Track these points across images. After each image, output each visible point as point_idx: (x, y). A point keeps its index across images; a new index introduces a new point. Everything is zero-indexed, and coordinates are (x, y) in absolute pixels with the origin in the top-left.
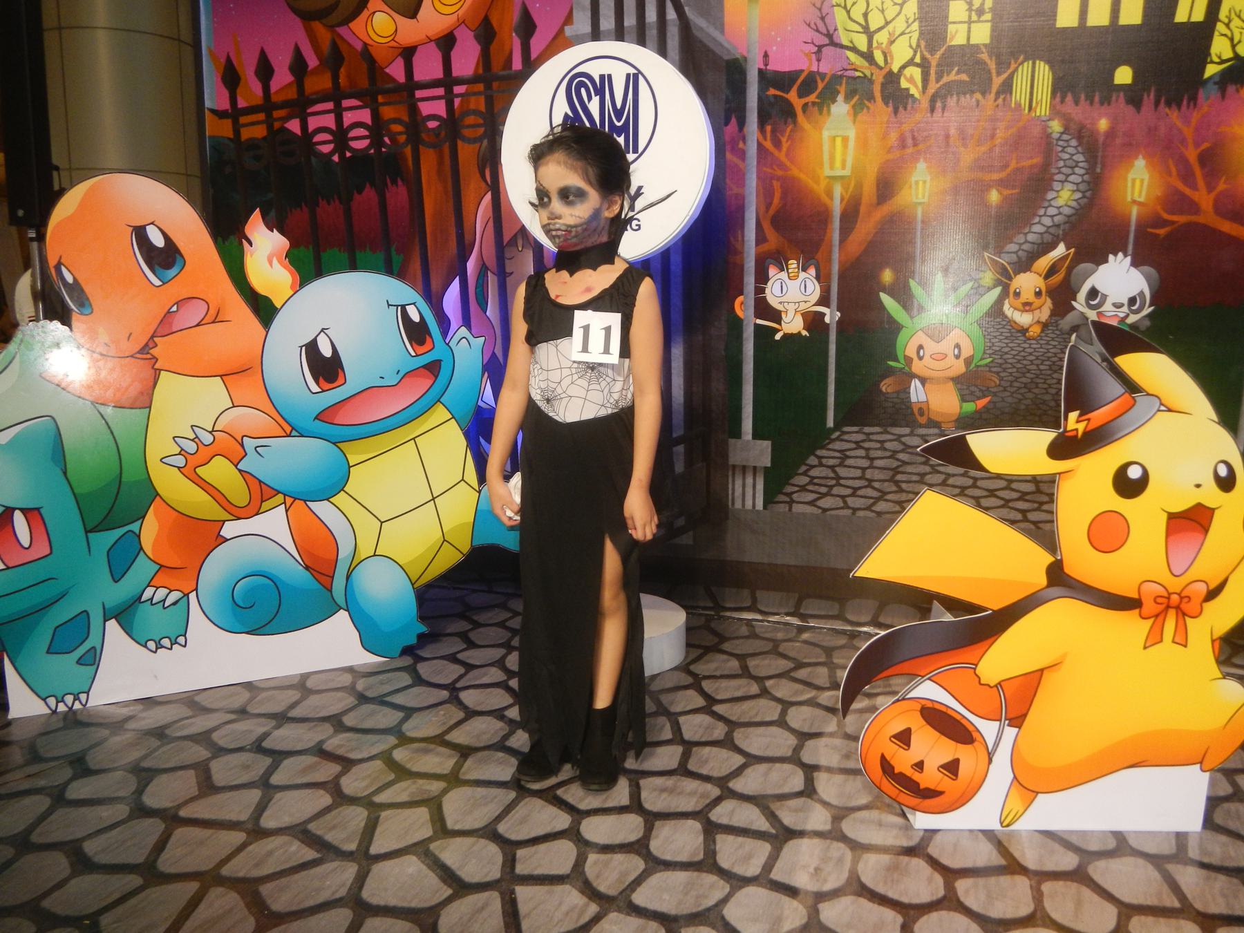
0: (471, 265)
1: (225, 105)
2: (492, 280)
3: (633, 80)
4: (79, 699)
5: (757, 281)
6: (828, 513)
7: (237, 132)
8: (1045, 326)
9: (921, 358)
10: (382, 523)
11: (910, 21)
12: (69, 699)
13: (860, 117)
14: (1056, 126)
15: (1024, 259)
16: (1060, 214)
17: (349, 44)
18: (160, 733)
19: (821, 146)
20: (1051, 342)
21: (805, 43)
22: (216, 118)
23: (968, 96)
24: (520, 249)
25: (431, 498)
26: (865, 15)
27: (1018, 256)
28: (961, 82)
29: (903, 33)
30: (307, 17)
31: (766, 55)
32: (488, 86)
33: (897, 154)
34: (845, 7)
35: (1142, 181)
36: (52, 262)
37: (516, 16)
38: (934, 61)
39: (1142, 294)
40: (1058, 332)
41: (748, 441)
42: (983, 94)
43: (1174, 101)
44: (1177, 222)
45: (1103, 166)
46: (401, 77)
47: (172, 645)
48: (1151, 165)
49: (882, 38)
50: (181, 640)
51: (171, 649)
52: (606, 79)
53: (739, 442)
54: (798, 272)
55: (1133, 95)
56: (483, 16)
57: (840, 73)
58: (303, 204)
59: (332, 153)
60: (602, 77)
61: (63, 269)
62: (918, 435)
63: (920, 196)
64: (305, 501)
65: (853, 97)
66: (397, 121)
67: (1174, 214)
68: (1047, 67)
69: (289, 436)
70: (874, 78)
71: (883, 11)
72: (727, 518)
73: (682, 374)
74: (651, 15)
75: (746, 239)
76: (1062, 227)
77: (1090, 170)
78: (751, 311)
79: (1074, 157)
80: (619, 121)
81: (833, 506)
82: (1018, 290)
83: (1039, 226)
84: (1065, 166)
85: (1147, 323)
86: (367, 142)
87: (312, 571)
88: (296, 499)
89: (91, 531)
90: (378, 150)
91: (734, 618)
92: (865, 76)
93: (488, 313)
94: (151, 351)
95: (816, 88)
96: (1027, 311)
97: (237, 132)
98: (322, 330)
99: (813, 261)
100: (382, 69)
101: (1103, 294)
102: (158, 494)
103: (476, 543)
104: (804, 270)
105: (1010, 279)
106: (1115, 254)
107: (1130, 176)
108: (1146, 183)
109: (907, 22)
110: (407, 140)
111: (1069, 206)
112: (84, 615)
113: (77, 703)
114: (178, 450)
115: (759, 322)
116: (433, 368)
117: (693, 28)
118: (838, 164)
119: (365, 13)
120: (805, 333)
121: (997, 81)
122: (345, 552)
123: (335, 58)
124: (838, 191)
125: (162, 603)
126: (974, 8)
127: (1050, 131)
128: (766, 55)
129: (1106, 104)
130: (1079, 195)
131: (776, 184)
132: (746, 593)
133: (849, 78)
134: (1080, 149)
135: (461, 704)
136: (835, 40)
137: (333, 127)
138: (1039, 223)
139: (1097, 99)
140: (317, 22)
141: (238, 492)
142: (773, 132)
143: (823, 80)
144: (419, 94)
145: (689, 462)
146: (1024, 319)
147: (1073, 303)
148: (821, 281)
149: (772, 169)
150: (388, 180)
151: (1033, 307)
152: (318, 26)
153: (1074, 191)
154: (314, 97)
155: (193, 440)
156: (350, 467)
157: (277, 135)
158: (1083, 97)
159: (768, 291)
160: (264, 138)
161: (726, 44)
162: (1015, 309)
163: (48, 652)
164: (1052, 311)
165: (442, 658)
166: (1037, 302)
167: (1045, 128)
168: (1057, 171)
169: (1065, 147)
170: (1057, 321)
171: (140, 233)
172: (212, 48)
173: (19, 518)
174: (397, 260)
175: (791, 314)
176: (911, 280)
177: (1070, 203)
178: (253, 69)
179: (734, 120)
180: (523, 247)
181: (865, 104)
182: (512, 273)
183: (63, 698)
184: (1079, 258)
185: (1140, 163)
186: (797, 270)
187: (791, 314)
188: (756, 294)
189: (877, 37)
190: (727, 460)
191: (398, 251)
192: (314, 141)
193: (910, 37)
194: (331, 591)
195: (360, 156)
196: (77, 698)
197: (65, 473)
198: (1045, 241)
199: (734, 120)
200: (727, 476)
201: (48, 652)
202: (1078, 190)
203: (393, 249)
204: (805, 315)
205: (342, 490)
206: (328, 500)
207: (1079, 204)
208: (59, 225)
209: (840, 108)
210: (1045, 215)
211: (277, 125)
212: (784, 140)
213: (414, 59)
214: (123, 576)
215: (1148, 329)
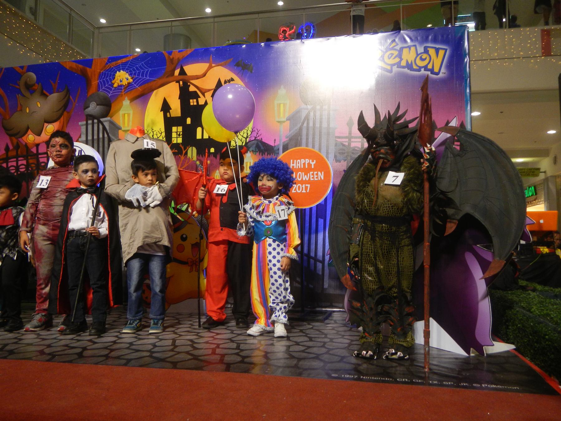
14: (198, 163)
26: (153, 136)
28: (176, 152)
30: (10, 136)
35: (218, 176)
42: (181, 155)
45: (209, 173)
46: (35, 152)
55: (215, 154)
59: (15, 172)
74: (101, 136)
86: (24, 169)
107: (216, 175)
119: (27, 135)
121: (184, 152)
123: (17, 147)
144: (40, 156)
150: (30, 180)
152: (14, 138)
195: (22, 173)
213: (39, 147)
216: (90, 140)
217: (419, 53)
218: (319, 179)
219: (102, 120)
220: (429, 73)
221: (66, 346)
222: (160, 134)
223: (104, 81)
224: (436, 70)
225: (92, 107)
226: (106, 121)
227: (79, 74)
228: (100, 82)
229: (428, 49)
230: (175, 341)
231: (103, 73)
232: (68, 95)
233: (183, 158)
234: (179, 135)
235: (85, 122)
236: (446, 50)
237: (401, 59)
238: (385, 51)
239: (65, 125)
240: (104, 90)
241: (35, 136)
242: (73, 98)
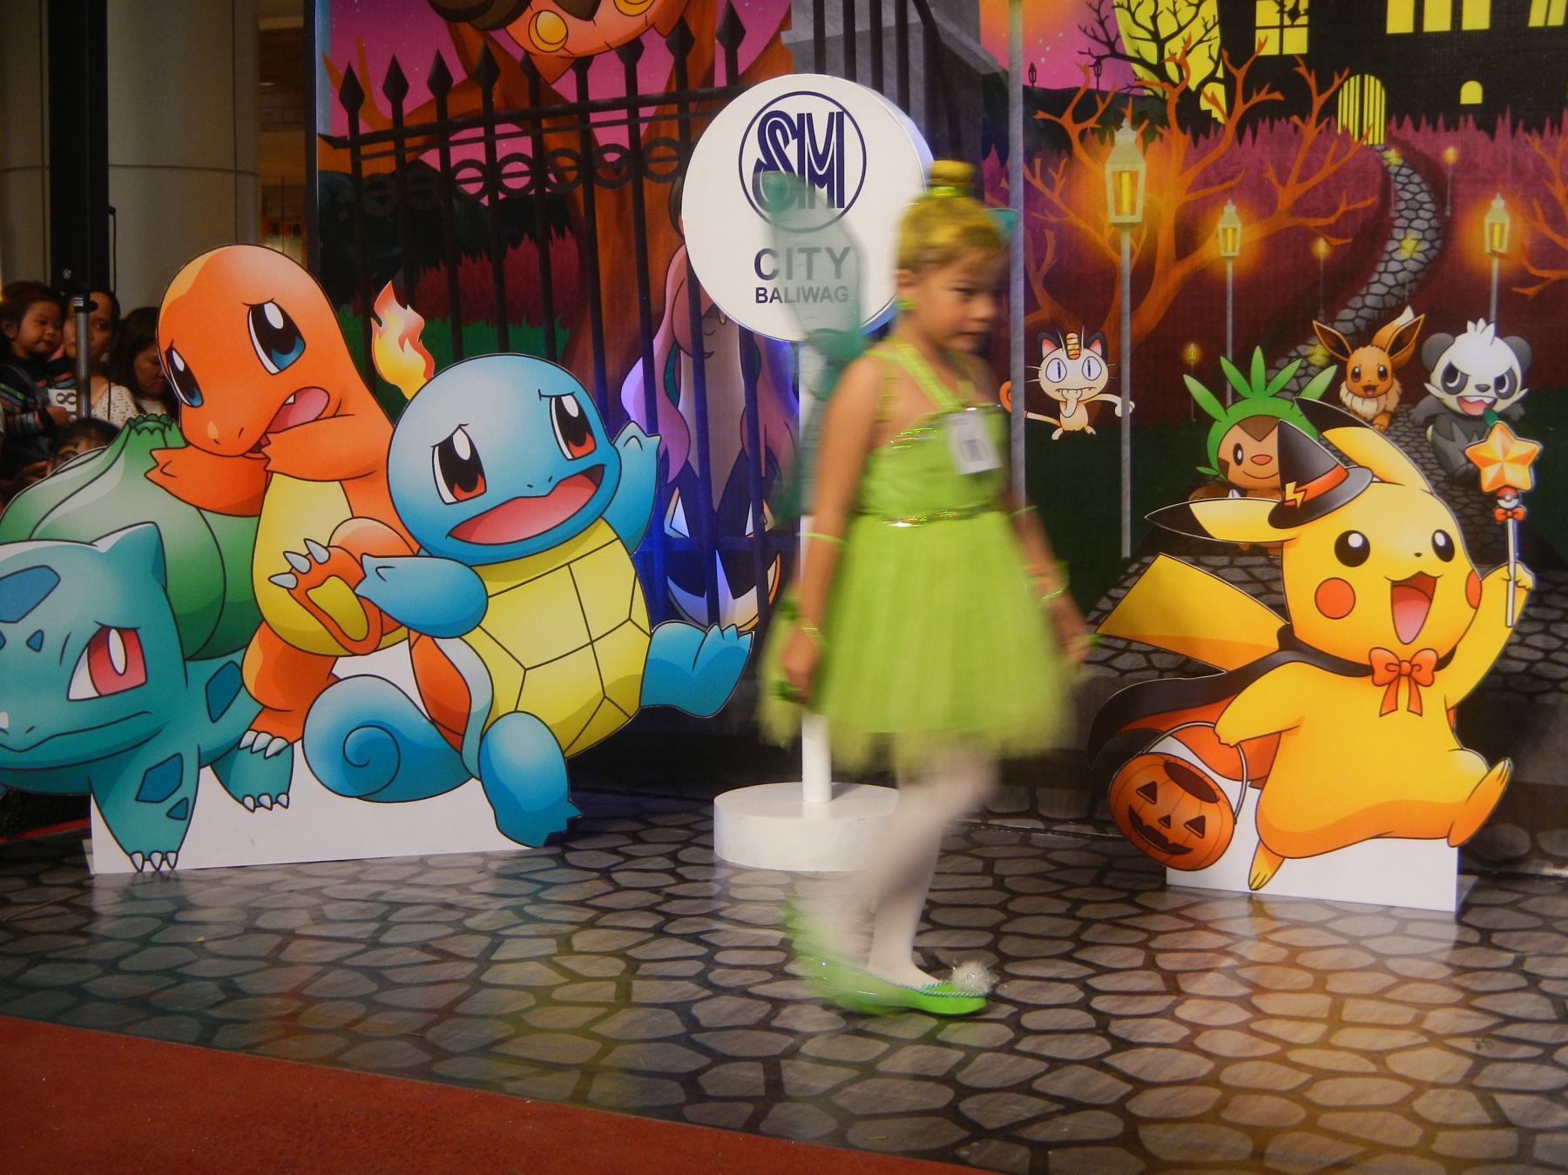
0: (658, 342)
1: (343, 130)
2: (686, 363)
3: (837, 120)
4: (167, 859)
5: (1028, 361)
6: (1128, 676)
7: (356, 165)
8: (1393, 416)
9: (1239, 462)
10: (526, 670)
11: (1209, 26)
12: (157, 858)
13: (1150, 145)
14: (1393, 157)
15: (1363, 328)
16: (1404, 269)
17: (506, 53)
18: (265, 887)
19: (1104, 185)
20: (1403, 438)
21: (1081, 53)
22: (329, 147)
23: (1283, 120)
25: (588, 641)
26: (1154, 18)
27: (1355, 325)
29: (1200, 41)
30: (453, 17)
31: (1032, 69)
32: (684, 107)
33: (1200, 194)
34: (1129, 9)
35: (1502, 226)
36: (164, 346)
37: (718, 18)
38: (1240, 74)
39: (1511, 372)
40: (1410, 425)
42: (1303, 119)
43: (1533, 126)
44: (1548, 279)
45: (1454, 210)
46: (571, 95)
47: (272, 804)
48: (1511, 206)
49: (1175, 46)
50: (283, 799)
51: (271, 809)
52: (806, 119)
54: (1079, 349)
55: (1485, 116)
56: (677, 18)
57: (1126, 91)
58: (441, 262)
59: (481, 194)
60: (801, 117)
61: (174, 353)
62: (1240, 567)
63: (1230, 247)
64: (433, 637)
65: (1141, 123)
66: (564, 152)
67: (1543, 268)
68: (1378, 83)
69: (414, 556)
70: (1167, 97)
71: (1175, 14)
74: (889, 18)
75: (1012, 306)
76: (1407, 286)
77: (1438, 213)
78: (1021, 402)
79: (1418, 197)
80: (821, 169)
81: (1134, 667)
82: (1357, 370)
83: (1378, 286)
84: (1407, 208)
85: (1520, 411)
86: (525, 181)
87: (440, 727)
88: (423, 633)
89: (191, 658)
90: (541, 191)
91: (1006, 828)
92: (1156, 94)
93: (680, 408)
94: (263, 450)
95: (1097, 109)
96: (1371, 397)
97: (356, 165)
98: (460, 427)
99: (1098, 334)
100: (548, 85)
101: (1462, 373)
102: (264, 619)
103: (648, 703)
104: (1087, 346)
105: (1347, 355)
106: (1476, 322)
107: (1488, 220)
108: (1507, 229)
109: (1205, 26)
110: (578, 177)
111: (1415, 260)
112: (177, 759)
113: (165, 863)
114: (288, 568)
115: (1031, 416)
116: (594, 475)
117: (940, 32)
118: (1126, 206)
119: (528, 13)
120: (1090, 430)
121: (1318, 102)
122: (479, 704)
123: (487, 71)
124: (1126, 242)
125: (263, 752)
126: (1287, 9)
127: (1386, 163)
128: (1032, 69)
129: (1452, 129)
130: (1425, 245)
131: (1049, 234)
133: (1133, 96)
134: (1424, 186)
135: (611, 880)
136: (1119, 51)
137: (482, 158)
138: (1378, 281)
139: (1441, 122)
140: (466, 24)
141: (353, 620)
142: (1043, 167)
143: (1104, 101)
144: (595, 117)
146: (1367, 407)
147: (1427, 385)
148: (1109, 358)
149: (1043, 214)
151: (1379, 390)
152: (467, 30)
153: (1419, 240)
154: (459, 120)
155: (305, 557)
156: (488, 597)
157: (409, 170)
158: (1424, 120)
159: (1041, 374)
160: (393, 174)
161: (984, 57)
162: (1355, 395)
163: (137, 799)
164: (1401, 397)
165: (600, 850)
166: (1382, 386)
167: (1380, 160)
168: (1398, 215)
169: (1405, 184)
170: (1407, 411)
171: (258, 312)
172: (328, 56)
173: (114, 638)
174: (562, 336)
175: (1072, 404)
176: (1222, 359)
177: (1416, 256)
178: (381, 83)
179: (994, 153)
181: (1158, 132)
182: (712, 353)
183: (150, 855)
184: (1428, 330)
185: (1498, 204)
186: (1077, 347)
187: (1072, 404)
188: (1026, 379)
189: (1169, 46)
191: (563, 327)
192: (457, 178)
193: (1210, 46)
194: (460, 753)
196: (164, 858)
197: (165, 589)
198: (1388, 306)
199: (994, 153)
201: (137, 799)
202: (1424, 239)
203: (557, 322)
204: (1090, 406)
205: (478, 625)
206: (460, 637)
207: (1426, 256)
208: (169, 308)
209: (1127, 136)
210: (1385, 271)
211: (409, 157)
212: (1057, 177)
213: (593, 74)
214: (222, 714)
215: (1522, 418)
216: (836, 38)
221: (1025, 1088)
222: (1193, 9)
230: (1493, 1100)
233: (1310, 130)
234: (1294, 14)
241: (569, 18)
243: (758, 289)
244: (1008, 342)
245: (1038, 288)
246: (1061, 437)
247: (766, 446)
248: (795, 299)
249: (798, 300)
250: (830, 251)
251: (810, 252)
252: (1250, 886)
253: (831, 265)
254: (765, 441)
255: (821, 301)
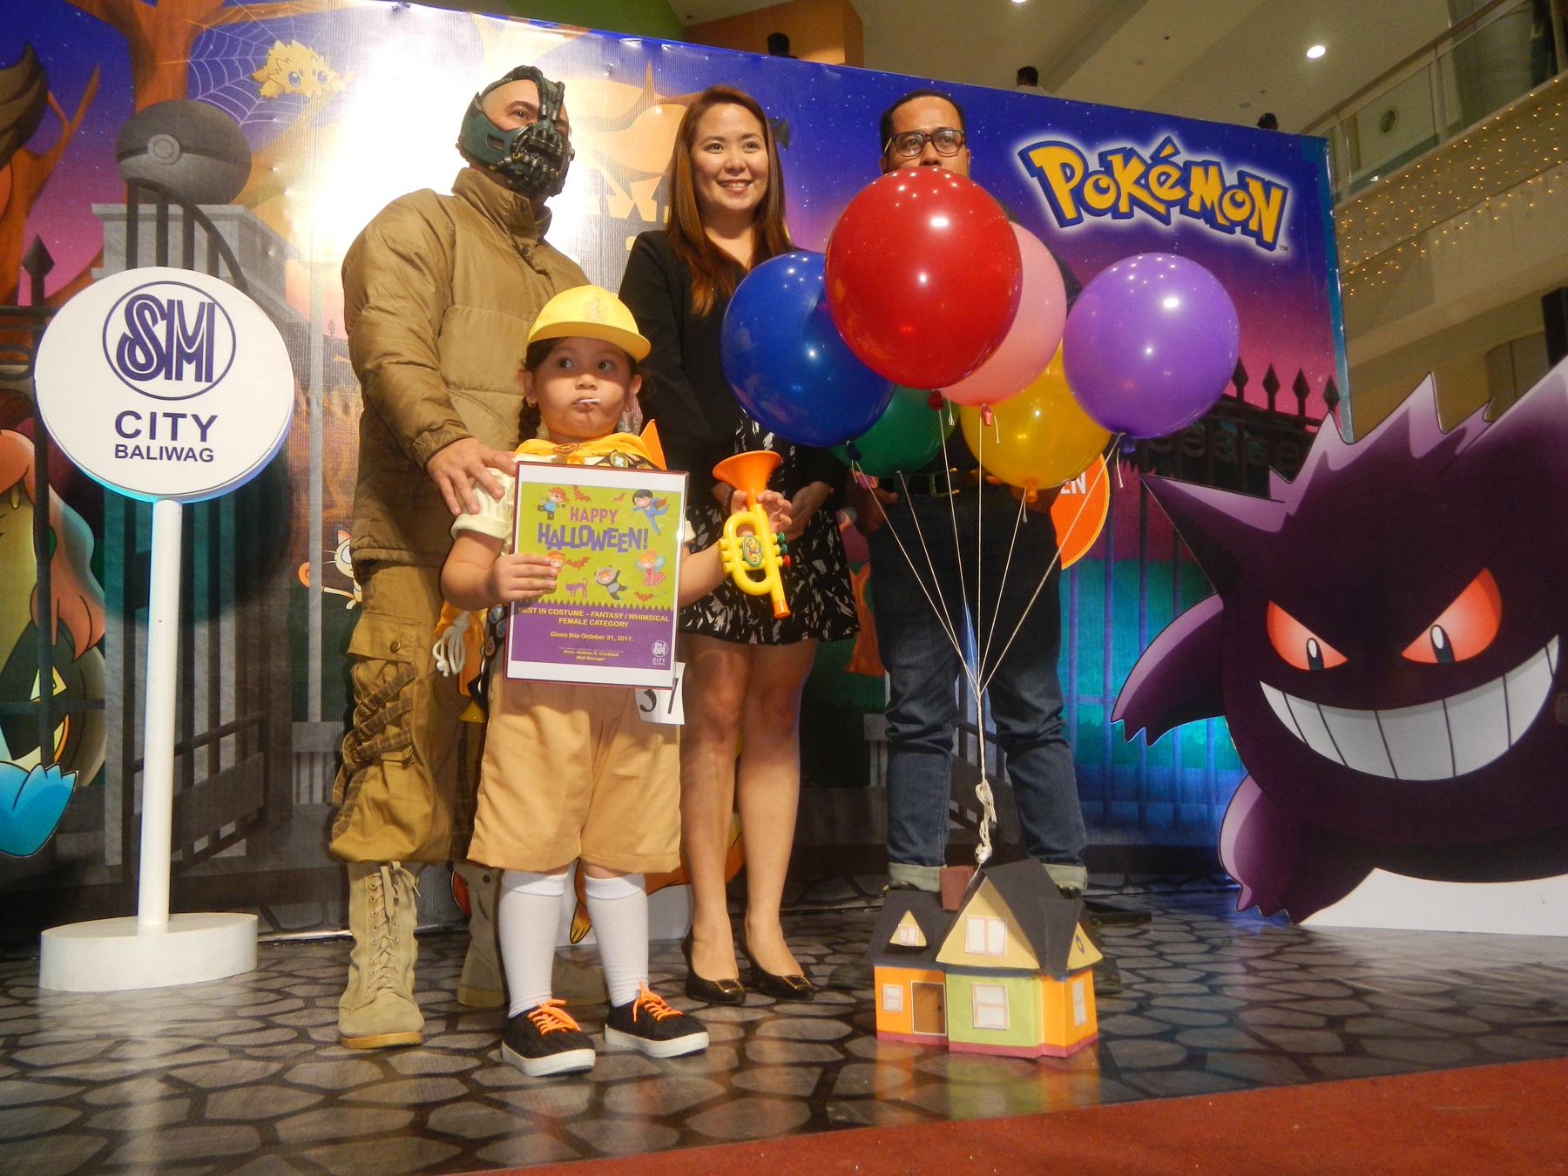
3: (209, 310)
24: (15, 506)
37: (25, 247)
41: (316, 724)
53: (305, 725)
60: (171, 303)
72: (290, 817)
73: (234, 651)
78: (318, 579)
80: (190, 348)
115: (327, 590)
132: (315, 906)
142: (342, 397)
145: (242, 753)
159: (337, 557)
180: (19, 504)
188: (324, 560)
190: (291, 748)
200: (291, 769)
217: (1227, 185)
218: (1074, 491)
219: (204, 208)
220: (1252, 241)
223: (214, 65)
224: (1268, 237)
225: (159, 152)
226: (225, 217)
227: (95, 14)
228: (199, 65)
229: (1248, 180)
231: (207, 30)
232: (36, 87)
235: (123, 208)
236: (1285, 190)
237: (1189, 194)
238: (1149, 161)
239: (19, 204)
240: (211, 96)
242: (60, 102)
243: (117, 446)
244: (307, 530)
245: (333, 489)
246: (354, 607)
247: (59, 619)
248: (158, 456)
249: (161, 458)
250: (196, 418)
251: (175, 417)
252: (571, 940)
253: (198, 431)
254: (58, 613)
255: (185, 460)
